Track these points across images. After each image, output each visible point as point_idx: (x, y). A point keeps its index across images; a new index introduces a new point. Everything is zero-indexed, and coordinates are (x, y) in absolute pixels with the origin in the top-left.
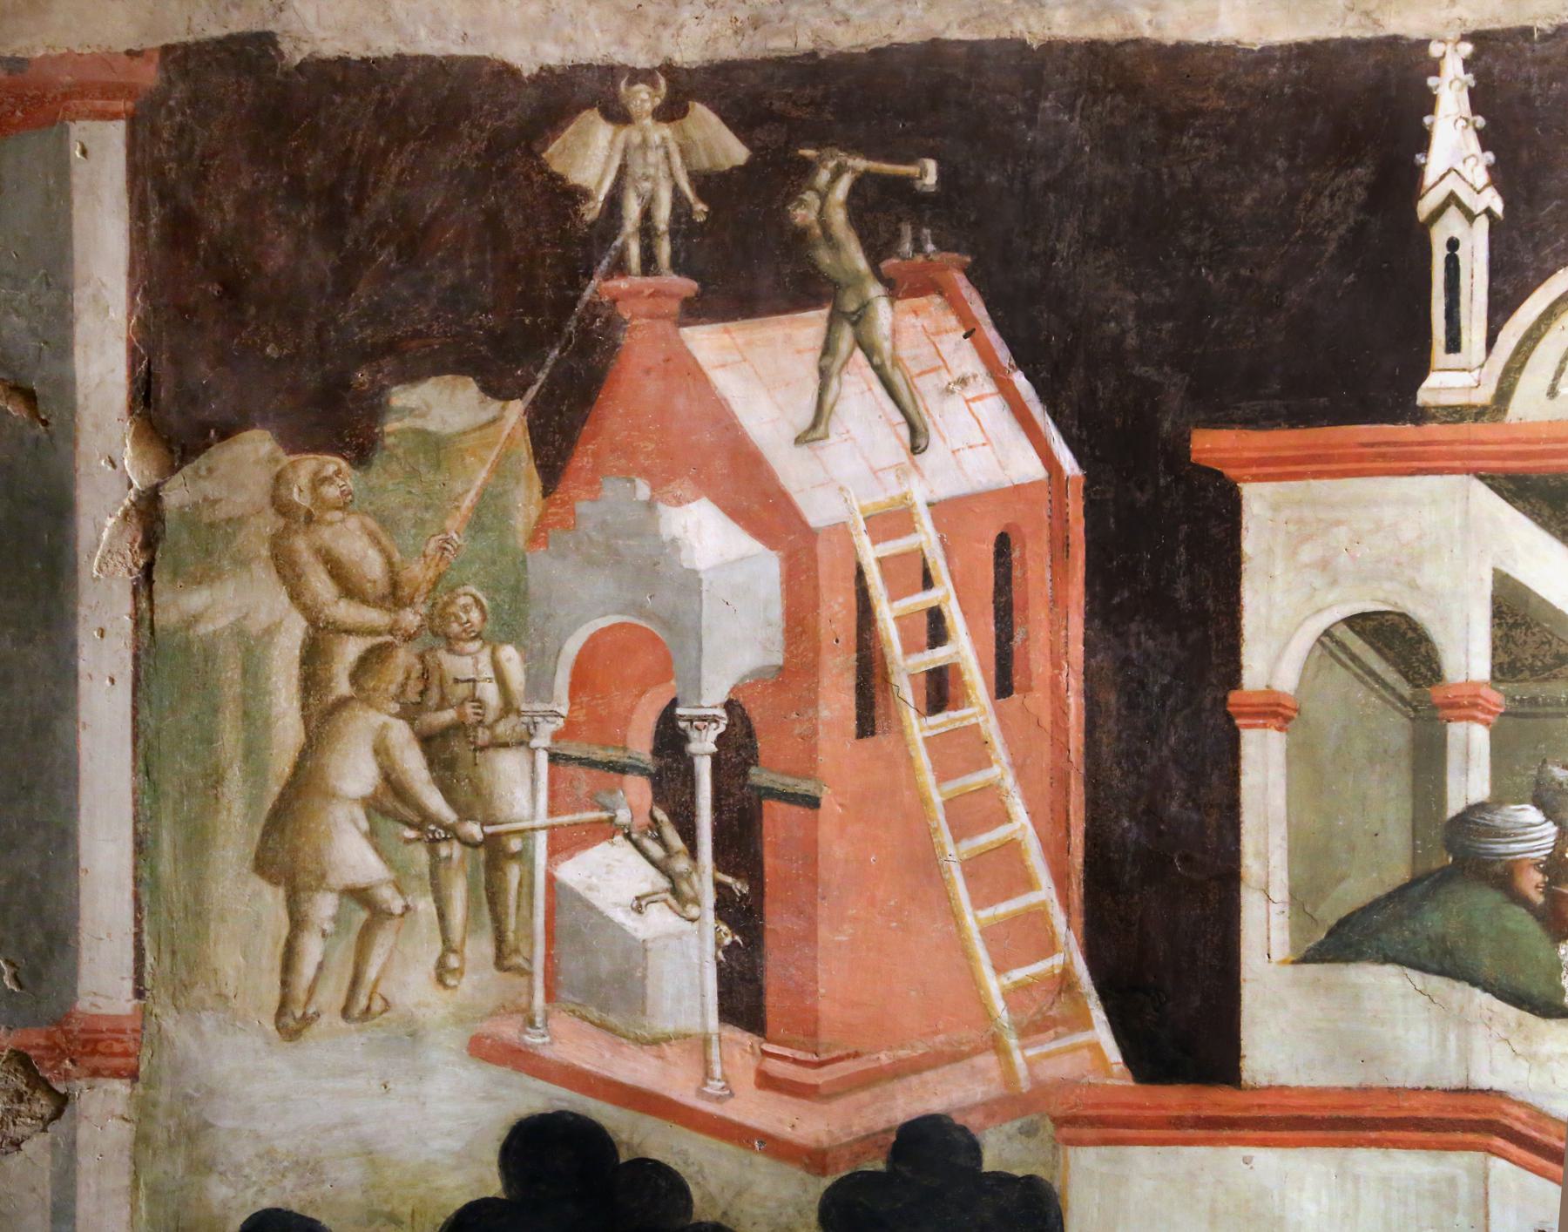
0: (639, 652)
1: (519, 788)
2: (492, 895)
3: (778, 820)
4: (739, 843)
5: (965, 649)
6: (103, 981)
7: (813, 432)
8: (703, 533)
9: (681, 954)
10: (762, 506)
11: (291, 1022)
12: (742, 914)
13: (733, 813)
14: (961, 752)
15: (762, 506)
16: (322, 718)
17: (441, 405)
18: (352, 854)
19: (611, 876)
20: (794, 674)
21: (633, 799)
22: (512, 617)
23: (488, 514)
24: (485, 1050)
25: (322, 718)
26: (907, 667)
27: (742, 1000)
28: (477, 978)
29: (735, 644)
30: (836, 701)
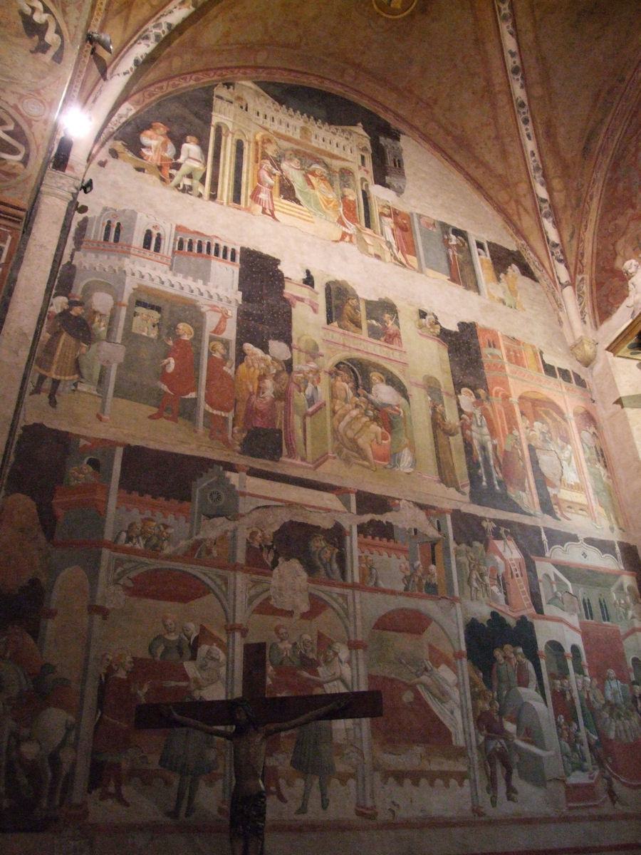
0: (494, 569)
1: (487, 579)
2: (486, 590)
3: (507, 586)
4: (505, 588)
5: (518, 572)
6: (457, 594)
7: (504, 551)
8: (498, 559)
9: (501, 596)
10: (502, 557)
11: (472, 600)
12: (505, 594)
13: (503, 583)
14: (519, 581)
15: (502, 557)
16: (471, 571)
17: (477, 544)
18: (475, 584)
19: (495, 589)
20: (506, 572)
21: (496, 582)
22: (485, 564)
23: (482, 555)
24: (487, 604)
25: (471, 571)
26: (515, 573)
27: (507, 602)
28: (486, 598)
29: (502, 570)
30: (510, 576)
